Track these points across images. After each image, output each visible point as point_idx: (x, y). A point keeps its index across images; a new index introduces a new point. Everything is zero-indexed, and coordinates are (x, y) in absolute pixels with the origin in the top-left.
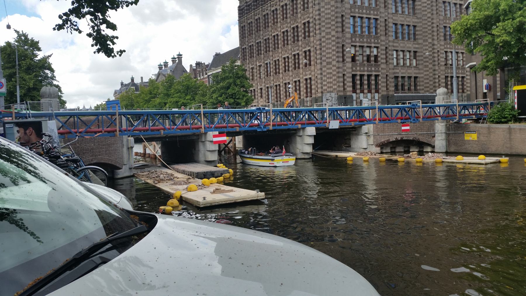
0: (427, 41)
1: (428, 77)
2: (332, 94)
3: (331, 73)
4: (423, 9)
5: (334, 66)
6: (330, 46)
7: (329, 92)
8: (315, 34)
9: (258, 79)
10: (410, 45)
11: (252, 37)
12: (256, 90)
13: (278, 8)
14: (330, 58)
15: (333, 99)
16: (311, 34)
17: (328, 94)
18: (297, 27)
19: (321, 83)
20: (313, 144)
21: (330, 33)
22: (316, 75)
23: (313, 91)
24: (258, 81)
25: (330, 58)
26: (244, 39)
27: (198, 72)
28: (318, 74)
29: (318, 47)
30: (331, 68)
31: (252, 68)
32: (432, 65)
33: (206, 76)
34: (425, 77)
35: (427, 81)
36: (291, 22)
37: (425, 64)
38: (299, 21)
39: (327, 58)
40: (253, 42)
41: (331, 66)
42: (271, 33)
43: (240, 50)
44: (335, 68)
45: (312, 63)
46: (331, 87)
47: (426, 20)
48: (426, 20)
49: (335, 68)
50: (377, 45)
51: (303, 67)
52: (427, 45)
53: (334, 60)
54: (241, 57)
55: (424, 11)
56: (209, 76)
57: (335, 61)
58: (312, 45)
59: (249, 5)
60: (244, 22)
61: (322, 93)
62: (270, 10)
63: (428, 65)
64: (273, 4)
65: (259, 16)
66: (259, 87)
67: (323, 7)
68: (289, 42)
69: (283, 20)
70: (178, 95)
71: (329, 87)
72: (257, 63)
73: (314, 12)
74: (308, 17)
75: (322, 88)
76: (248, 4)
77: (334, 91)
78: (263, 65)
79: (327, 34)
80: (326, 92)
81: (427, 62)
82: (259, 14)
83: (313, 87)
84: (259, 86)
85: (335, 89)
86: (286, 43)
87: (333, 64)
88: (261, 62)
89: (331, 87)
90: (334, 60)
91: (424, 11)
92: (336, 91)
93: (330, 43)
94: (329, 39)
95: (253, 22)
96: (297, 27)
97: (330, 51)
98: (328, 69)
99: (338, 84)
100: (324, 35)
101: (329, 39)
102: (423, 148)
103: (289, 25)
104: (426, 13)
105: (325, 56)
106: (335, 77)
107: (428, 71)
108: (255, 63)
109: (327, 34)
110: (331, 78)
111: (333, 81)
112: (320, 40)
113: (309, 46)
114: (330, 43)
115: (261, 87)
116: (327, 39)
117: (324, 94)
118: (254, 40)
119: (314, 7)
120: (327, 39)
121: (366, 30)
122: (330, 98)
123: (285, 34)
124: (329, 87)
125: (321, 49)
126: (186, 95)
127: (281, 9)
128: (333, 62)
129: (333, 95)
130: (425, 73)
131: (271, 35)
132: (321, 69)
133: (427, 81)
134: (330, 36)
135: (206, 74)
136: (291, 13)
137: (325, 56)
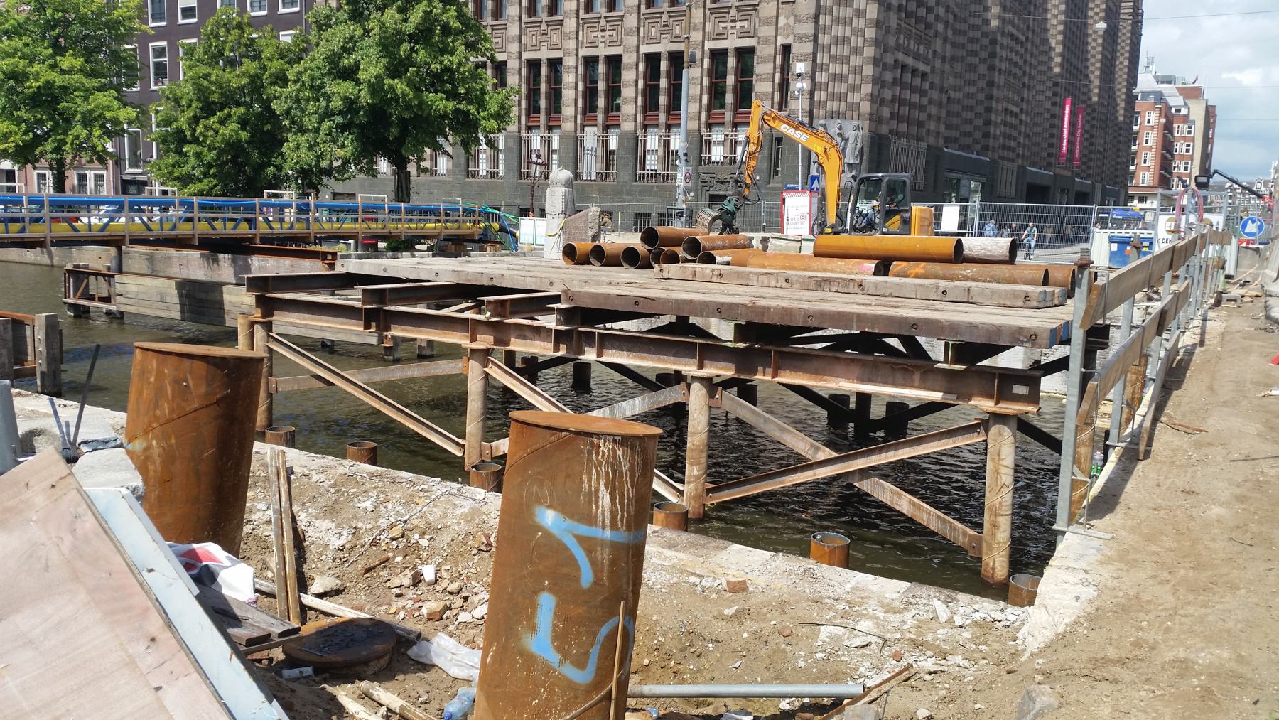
1: (971, 102)
3: (845, 41)
7: (832, 115)
28: (799, 38)
30: (846, 22)
34: (966, 102)
35: (969, 115)
37: (970, 60)
46: (841, 97)
51: (642, 7)
63: (976, 66)
70: (17, 43)
71: (833, 97)
80: (822, 113)
81: (975, 54)
85: (853, 107)
89: (841, 97)
98: (838, 21)
99: (926, 85)
110: (844, 60)
124: (833, 97)
126: (59, 50)
133: (969, 115)
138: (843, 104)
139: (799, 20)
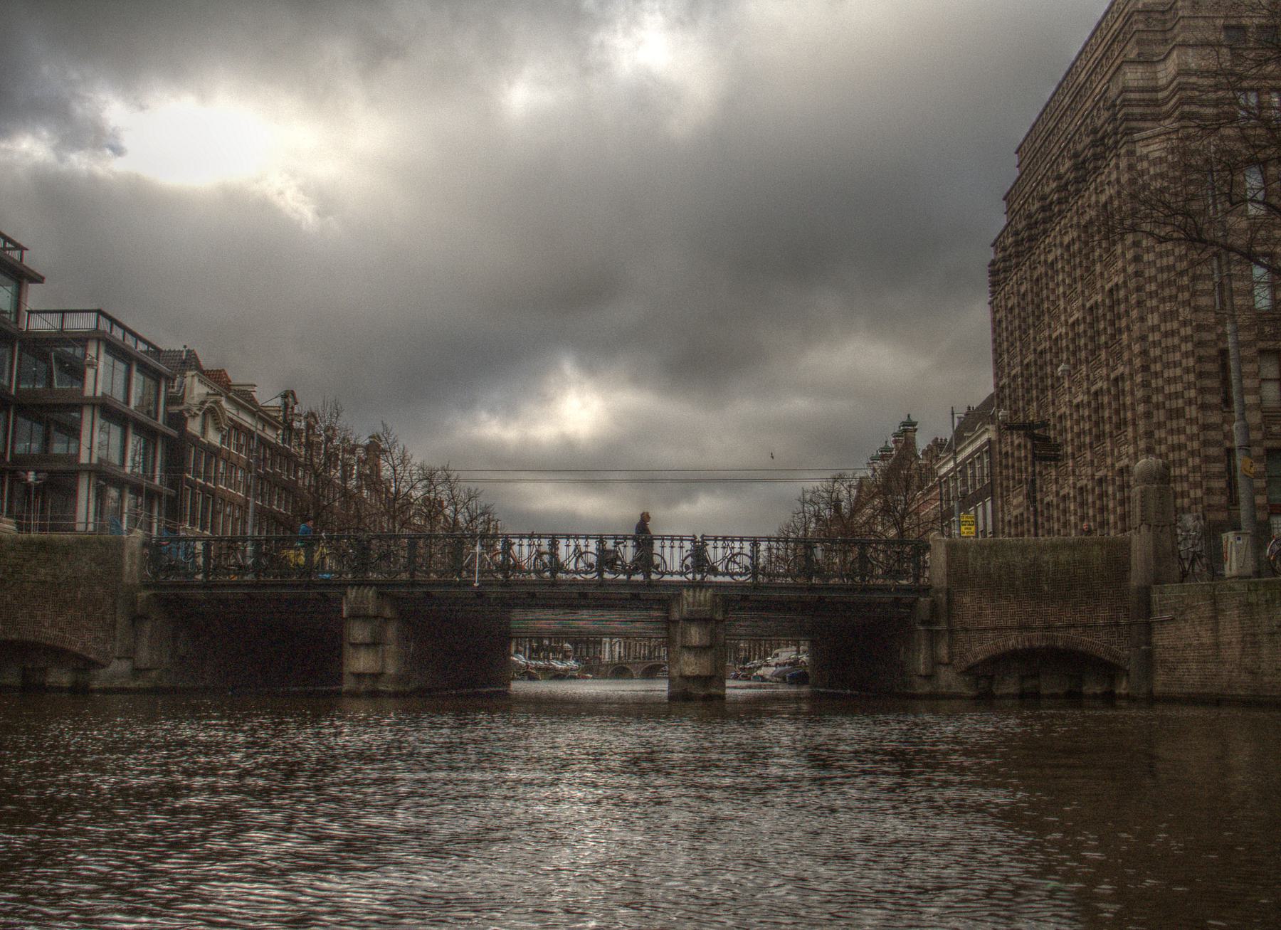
5: (1191, 421)
6: (1178, 356)
14: (1177, 395)
30: (1180, 431)
39: (1170, 397)
41: (1182, 422)
44: (1195, 429)
49: (1195, 429)
79: (1165, 317)
85: (1195, 501)
90: (1190, 402)
92: (1200, 507)
93: (1175, 348)
94: (1173, 333)
97: (1178, 371)
98: (1172, 432)
100: (1156, 322)
101: (1173, 333)
111: (1189, 472)
114: (1175, 348)
116: (1166, 335)
120: (1166, 335)
128: (1187, 408)
134: (1175, 325)
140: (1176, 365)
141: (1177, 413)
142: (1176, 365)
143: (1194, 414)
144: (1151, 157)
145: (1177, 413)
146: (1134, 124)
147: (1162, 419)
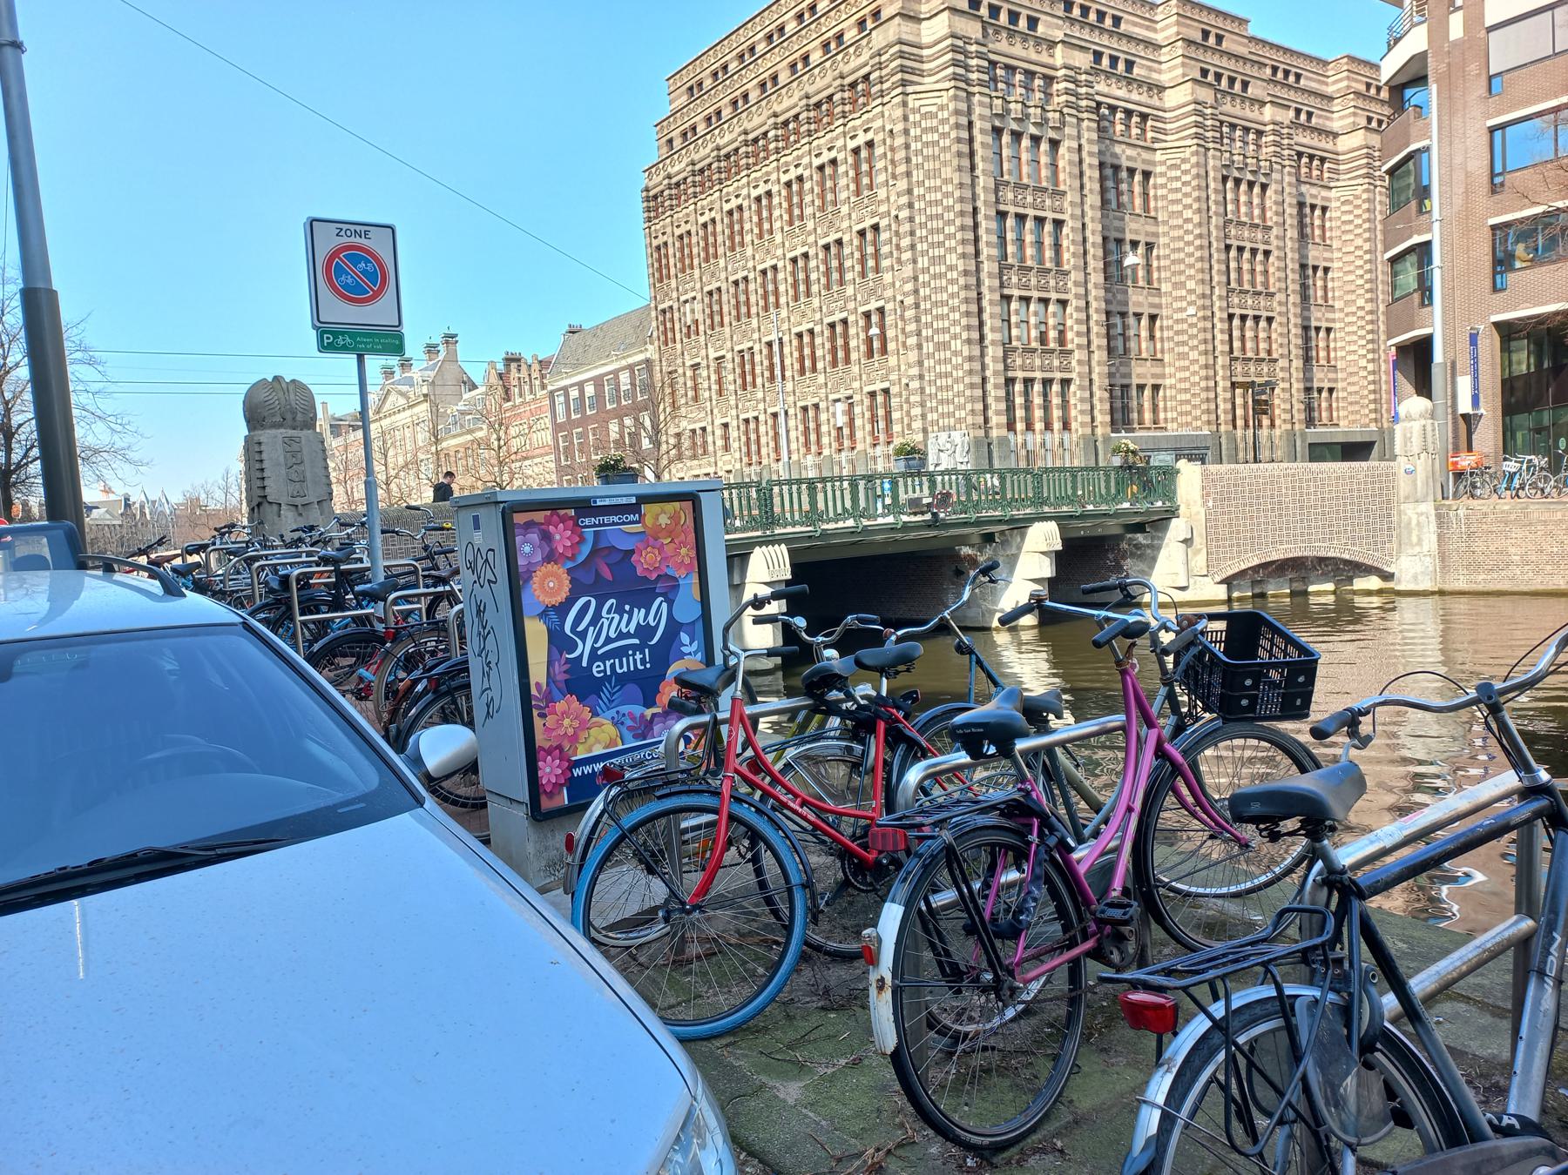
0: (1182, 285)
2: (953, 433)
4: (1170, 197)
5: (955, 353)
8: (899, 261)
9: (714, 397)
10: (1141, 299)
11: (691, 275)
12: (709, 429)
13: (775, 189)
14: (945, 330)
15: (959, 449)
16: (885, 263)
17: (943, 436)
18: (839, 242)
19: (923, 405)
20: (1049, 579)
21: (942, 259)
22: (904, 381)
23: (896, 428)
24: (714, 402)
25: (945, 330)
26: (665, 281)
27: (515, 382)
29: (909, 301)
30: (947, 361)
31: (696, 367)
32: (1196, 353)
33: (541, 393)
36: (819, 230)
38: (845, 224)
39: (937, 331)
40: (693, 289)
42: (753, 259)
43: (653, 314)
45: (891, 346)
47: (1180, 227)
48: (1180, 227)
50: (1063, 296)
52: (1182, 298)
53: (955, 337)
54: (655, 334)
55: (1173, 202)
56: (552, 392)
57: (959, 341)
58: (889, 293)
59: (678, 185)
60: (664, 234)
61: (925, 431)
62: (749, 196)
64: (756, 179)
65: (713, 214)
66: (718, 422)
67: (920, 184)
68: (815, 288)
69: (791, 223)
72: (711, 350)
73: (892, 199)
74: (874, 214)
75: (924, 416)
76: (674, 180)
77: (958, 426)
78: (729, 356)
79: (934, 261)
80: (936, 428)
81: (1184, 343)
82: (710, 210)
83: (896, 415)
84: (719, 416)
85: (959, 421)
86: (801, 288)
87: (953, 348)
88: (721, 348)
90: (955, 337)
91: (1173, 202)
92: (963, 426)
93: (943, 289)
94: (941, 276)
95: (693, 232)
96: (839, 242)
101: (941, 276)
102: (1350, 580)
103: (811, 239)
104: (1180, 208)
105: (929, 325)
106: (961, 387)
107: (1187, 368)
108: (703, 352)
109: (934, 261)
112: (916, 279)
113: (880, 298)
114: (943, 289)
115: (724, 421)
116: (935, 277)
117: (931, 435)
118: (698, 286)
119: (891, 183)
121: (1030, 251)
122: (948, 446)
123: (801, 263)
125: (917, 306)
127: (784, 193)
128: (953, 342)
129: (957, 436)
130: (1179, 375)
131: (755, 267)
132: (920, 363)
135: (543, 387)
136: (817, 203)
137: (929, 325)
138: (952, 420)
139: (910, 367)
140: (943, 304)
141: (944, 346)
142: (943, 304)
143: (1193, 287)
144: (923, 110)
145: (944, 346)
146: (907, 77)
147: (931, 350)
